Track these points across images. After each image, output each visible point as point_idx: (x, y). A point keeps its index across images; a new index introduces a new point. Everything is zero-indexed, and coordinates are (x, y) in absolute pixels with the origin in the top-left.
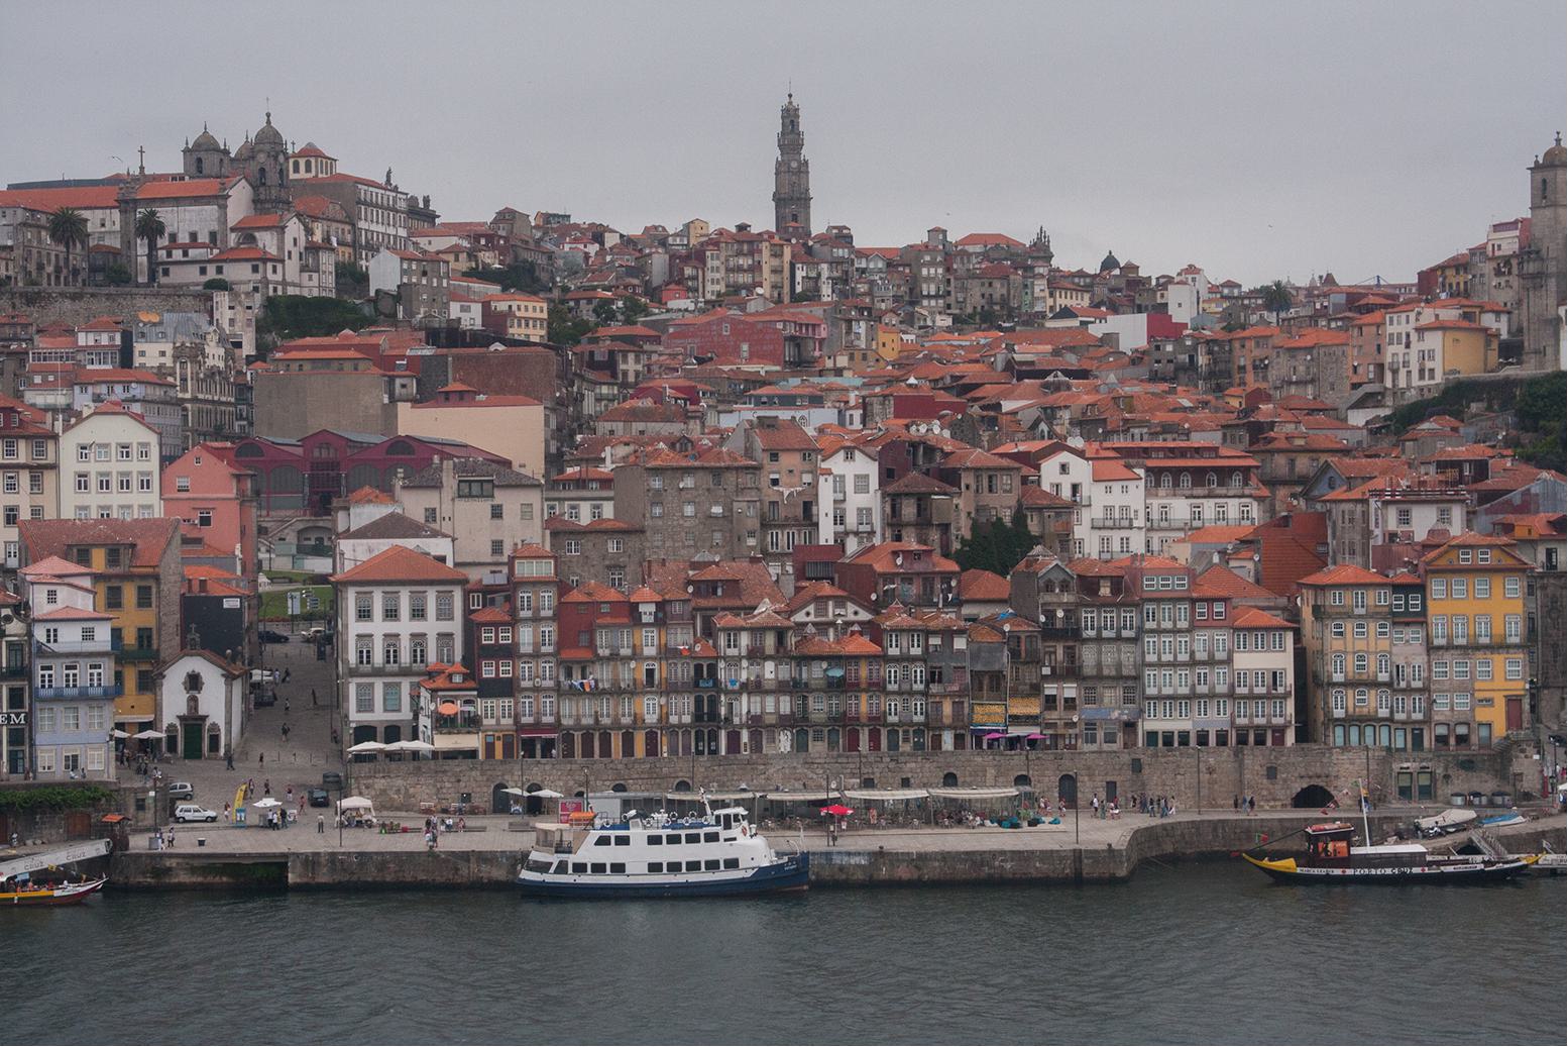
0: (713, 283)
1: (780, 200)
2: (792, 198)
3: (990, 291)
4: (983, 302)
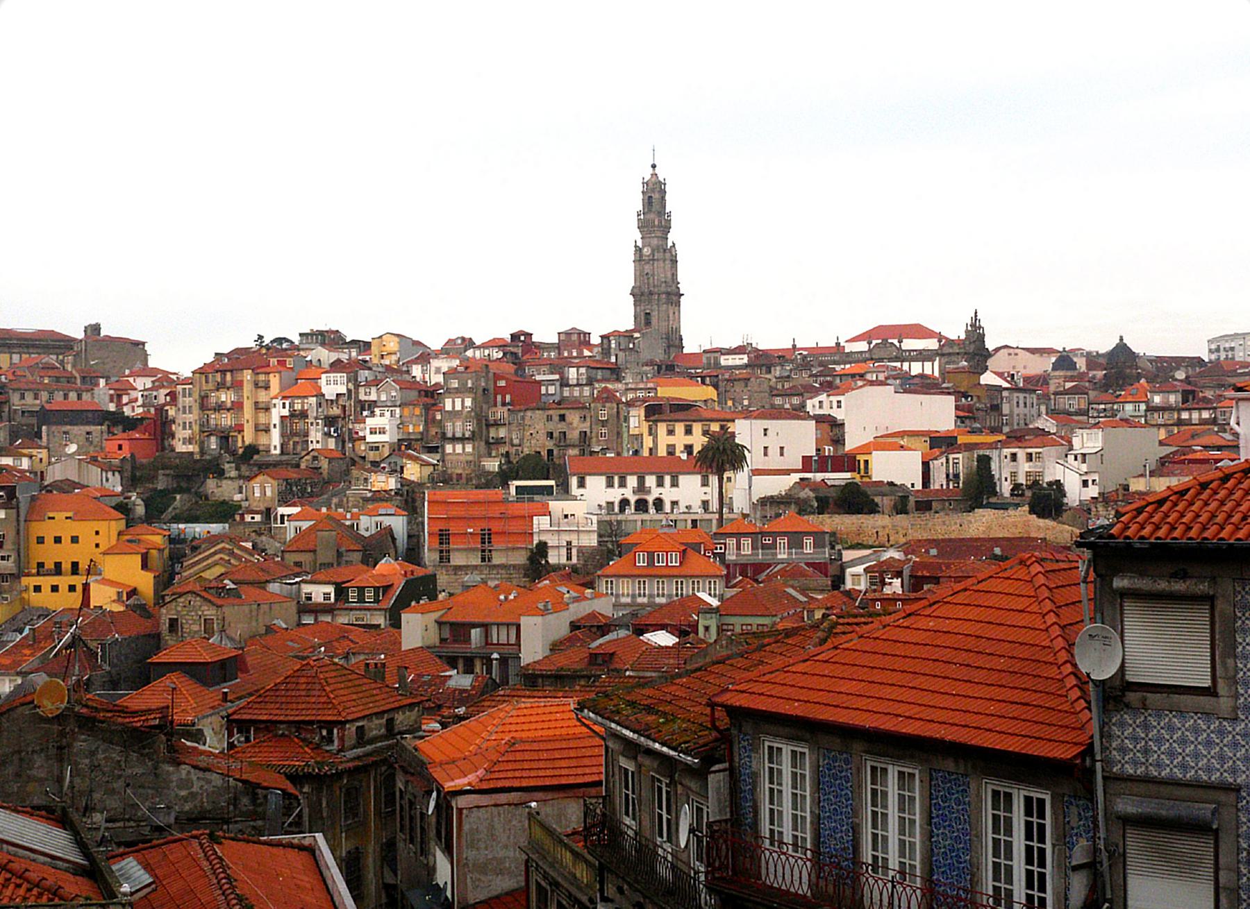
0: (184, 428)
1: (639, 295)
2: (657, 289)
3: (562, 427)
4: (550, 444)
